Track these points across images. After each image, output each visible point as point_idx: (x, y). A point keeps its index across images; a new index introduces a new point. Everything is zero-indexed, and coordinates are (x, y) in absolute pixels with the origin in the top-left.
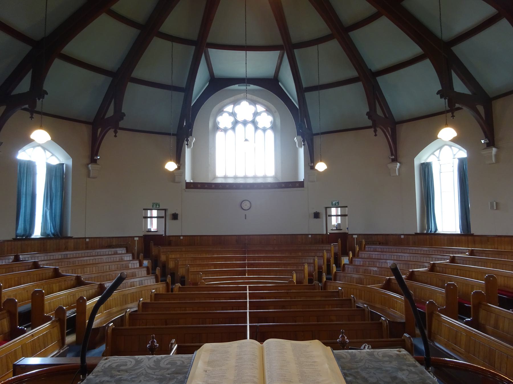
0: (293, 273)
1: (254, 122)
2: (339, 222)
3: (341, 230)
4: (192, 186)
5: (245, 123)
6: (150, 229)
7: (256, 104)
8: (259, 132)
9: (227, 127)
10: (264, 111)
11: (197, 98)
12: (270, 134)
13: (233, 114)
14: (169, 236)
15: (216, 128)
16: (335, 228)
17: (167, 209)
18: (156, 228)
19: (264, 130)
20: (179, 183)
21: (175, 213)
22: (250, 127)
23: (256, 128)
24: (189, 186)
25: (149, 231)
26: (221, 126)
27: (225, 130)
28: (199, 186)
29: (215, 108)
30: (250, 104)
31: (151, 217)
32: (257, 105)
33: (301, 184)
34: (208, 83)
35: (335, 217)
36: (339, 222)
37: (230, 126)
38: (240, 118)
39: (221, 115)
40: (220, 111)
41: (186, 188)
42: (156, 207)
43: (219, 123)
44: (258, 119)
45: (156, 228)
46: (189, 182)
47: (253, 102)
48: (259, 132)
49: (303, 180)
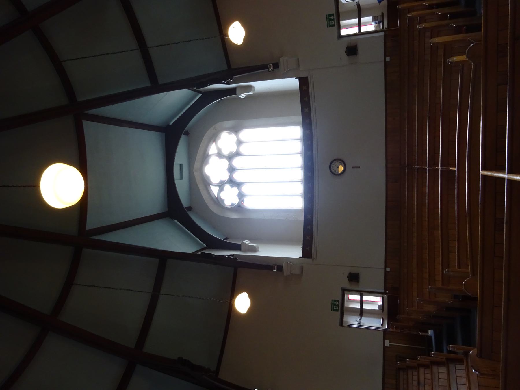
0: (451, 62)
1: (230, 158)
2: (369, 19)
3: (383, 14)
4: (308, 248)
5: (232, 170)
6: (379, 306)
7: (208, 155)
8: (243, 149)
9: (237, 194)
10: (216, 144)
11: (193, 235)
12: (246, 134)
13: (221, 185)
14: (385, 289)
15: (239, 208)
16: (381, 25)
17: (342, 288)
18: (379, 298)
19: (240, 143)
20: (302, 268)
21: (348, 277)
22: (237, 162)
23: (238, 154)
24: (307, 253)
25: (382, 308)
26: (236, 201)
27: (241, 196)
28: (308, 238)
29: (213, 210)
30: (207, 163)
31: (361, 302)
32: (209, 154)
33: (303, 82)
34: (174, 220)
35: (362, 28)
36: (369, 19)
37: (235, 190)
38: (225, 177)
39: (223, 201)
40: (218, 202)
41: (311, 258)
42: (338, 305)
43: (232, 205)
44: (226, 152)
45: (379, 297)
46: (301, 252)
47: (205, 158)
48: (242, 149)
49: (298, 80)
